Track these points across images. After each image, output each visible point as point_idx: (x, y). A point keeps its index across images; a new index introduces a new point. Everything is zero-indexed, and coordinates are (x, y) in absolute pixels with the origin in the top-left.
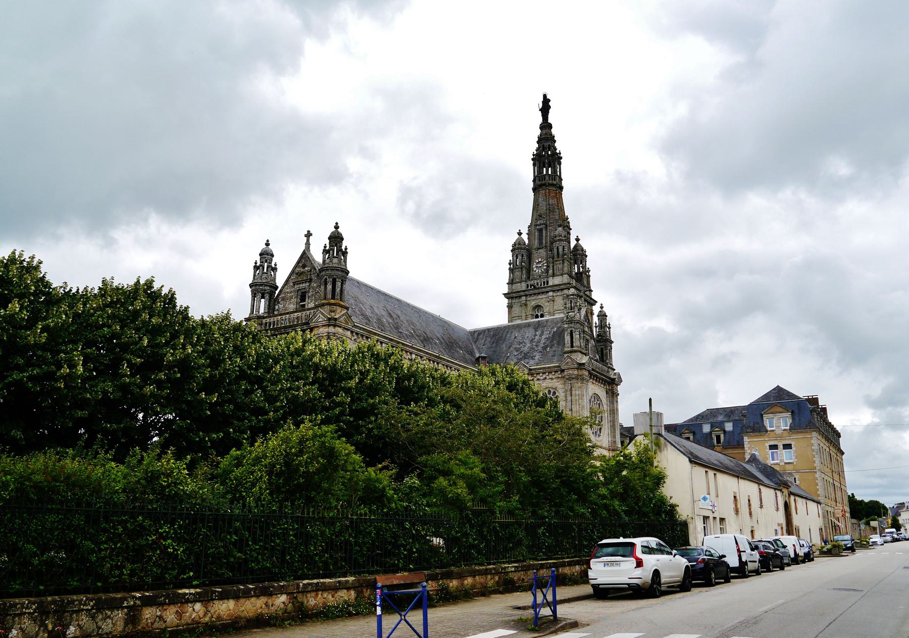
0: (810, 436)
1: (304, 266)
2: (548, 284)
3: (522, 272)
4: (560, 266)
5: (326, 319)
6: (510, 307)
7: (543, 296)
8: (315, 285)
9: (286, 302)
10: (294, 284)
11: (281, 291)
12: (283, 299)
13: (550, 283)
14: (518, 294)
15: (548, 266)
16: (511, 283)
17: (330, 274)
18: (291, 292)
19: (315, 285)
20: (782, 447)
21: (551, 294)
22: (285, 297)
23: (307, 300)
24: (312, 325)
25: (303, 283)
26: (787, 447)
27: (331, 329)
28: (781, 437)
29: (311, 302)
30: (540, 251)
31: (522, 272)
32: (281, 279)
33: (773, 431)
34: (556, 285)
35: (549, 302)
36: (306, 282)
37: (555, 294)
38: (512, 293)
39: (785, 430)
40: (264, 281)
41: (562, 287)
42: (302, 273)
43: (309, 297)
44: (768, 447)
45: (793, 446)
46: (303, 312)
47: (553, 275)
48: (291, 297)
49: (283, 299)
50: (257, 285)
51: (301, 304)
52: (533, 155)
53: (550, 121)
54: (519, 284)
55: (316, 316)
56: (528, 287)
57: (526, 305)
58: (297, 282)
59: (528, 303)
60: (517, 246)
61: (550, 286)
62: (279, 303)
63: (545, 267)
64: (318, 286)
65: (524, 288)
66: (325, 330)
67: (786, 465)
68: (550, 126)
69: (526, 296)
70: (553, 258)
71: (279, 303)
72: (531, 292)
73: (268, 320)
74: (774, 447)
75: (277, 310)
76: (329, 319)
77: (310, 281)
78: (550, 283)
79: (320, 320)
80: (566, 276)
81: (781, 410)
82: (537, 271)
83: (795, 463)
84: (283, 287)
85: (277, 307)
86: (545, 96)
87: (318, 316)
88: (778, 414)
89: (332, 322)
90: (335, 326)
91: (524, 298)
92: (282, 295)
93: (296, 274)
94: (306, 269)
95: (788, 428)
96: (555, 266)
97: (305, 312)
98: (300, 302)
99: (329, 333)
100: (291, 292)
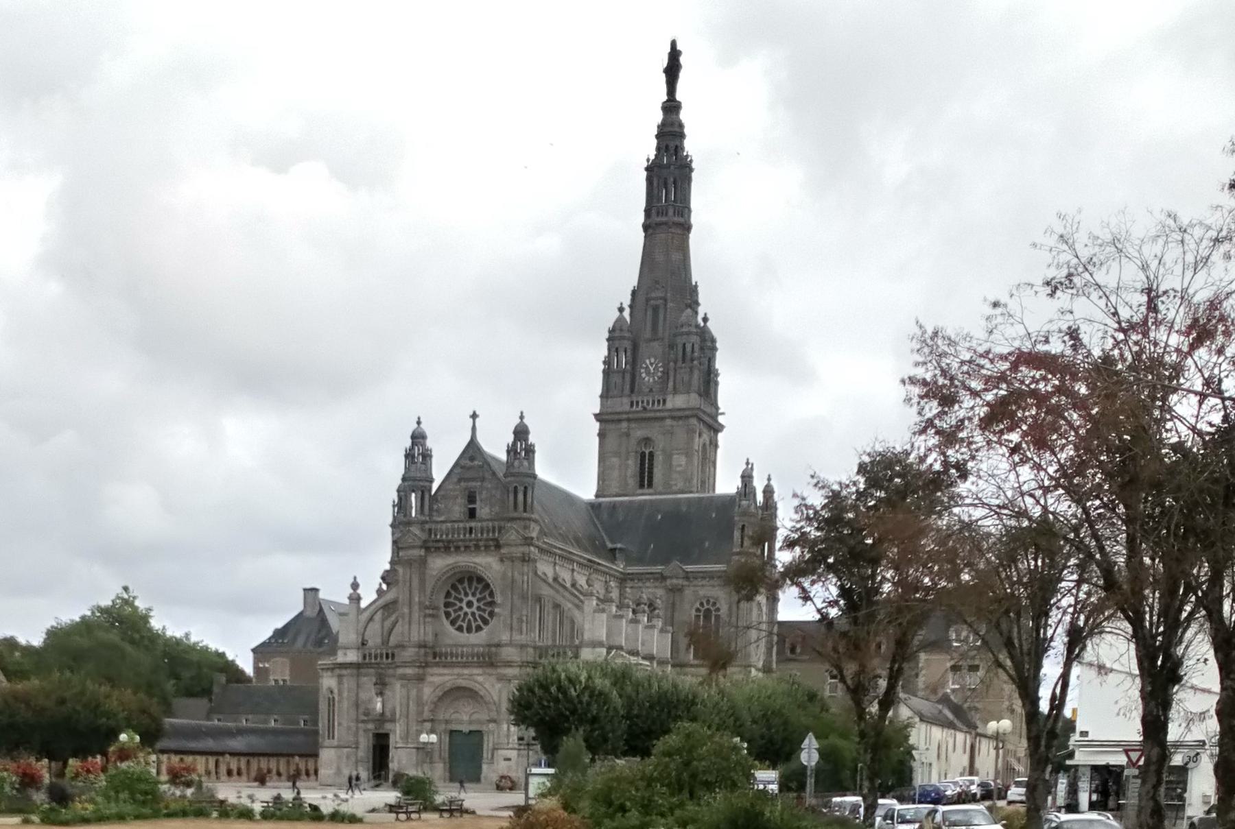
1: (472, 459)
2: (664, 401)
3: (623, 378)
4: (686, 378)
6: (602, 435)
7: (657, 424)
10: (460, 480)
11: (440, 487)
12: (444, 497)
13: (669, 405)
14: (616, 417)
15: (666, 373)
16: (604, 396)
21: (669, 422)
23: (478, 503)
27: (525, 549)
30: (653, 344)
31: (623, 378)
32: (440, 470)
34: (679, 410)
35: (664, 434)
37: (675, 423)
38: (608, 414)
40: (424, 475)
41: (687, 413)
42: (470, 468)
47: (675, 391)
49: (444, 497)
54: (619, 399)
56: (632, 405)
57: (628, 435)
59: (632, 432)
60: (617, 334)
61: (670, 410)
62: (437, 501)
63: (659, 374)
65: (627, 408)
69: (629, 420)
70: (675, 362)
71: (437, 501)
72: (636, 416)
73: (433, 526)
75: (437, 511)
76: (526, 538)
77: (483, 479)
78: (669, 405)
79: (513, 537)
80: (694, 396)
82: (646, 379)
85: (435, 507)
89: (528, 541)
90: (529, 545)
91: (624, 425)
92: (442, 493)
96: (678, 376)
99: (523, 554)
100: (455, 490)
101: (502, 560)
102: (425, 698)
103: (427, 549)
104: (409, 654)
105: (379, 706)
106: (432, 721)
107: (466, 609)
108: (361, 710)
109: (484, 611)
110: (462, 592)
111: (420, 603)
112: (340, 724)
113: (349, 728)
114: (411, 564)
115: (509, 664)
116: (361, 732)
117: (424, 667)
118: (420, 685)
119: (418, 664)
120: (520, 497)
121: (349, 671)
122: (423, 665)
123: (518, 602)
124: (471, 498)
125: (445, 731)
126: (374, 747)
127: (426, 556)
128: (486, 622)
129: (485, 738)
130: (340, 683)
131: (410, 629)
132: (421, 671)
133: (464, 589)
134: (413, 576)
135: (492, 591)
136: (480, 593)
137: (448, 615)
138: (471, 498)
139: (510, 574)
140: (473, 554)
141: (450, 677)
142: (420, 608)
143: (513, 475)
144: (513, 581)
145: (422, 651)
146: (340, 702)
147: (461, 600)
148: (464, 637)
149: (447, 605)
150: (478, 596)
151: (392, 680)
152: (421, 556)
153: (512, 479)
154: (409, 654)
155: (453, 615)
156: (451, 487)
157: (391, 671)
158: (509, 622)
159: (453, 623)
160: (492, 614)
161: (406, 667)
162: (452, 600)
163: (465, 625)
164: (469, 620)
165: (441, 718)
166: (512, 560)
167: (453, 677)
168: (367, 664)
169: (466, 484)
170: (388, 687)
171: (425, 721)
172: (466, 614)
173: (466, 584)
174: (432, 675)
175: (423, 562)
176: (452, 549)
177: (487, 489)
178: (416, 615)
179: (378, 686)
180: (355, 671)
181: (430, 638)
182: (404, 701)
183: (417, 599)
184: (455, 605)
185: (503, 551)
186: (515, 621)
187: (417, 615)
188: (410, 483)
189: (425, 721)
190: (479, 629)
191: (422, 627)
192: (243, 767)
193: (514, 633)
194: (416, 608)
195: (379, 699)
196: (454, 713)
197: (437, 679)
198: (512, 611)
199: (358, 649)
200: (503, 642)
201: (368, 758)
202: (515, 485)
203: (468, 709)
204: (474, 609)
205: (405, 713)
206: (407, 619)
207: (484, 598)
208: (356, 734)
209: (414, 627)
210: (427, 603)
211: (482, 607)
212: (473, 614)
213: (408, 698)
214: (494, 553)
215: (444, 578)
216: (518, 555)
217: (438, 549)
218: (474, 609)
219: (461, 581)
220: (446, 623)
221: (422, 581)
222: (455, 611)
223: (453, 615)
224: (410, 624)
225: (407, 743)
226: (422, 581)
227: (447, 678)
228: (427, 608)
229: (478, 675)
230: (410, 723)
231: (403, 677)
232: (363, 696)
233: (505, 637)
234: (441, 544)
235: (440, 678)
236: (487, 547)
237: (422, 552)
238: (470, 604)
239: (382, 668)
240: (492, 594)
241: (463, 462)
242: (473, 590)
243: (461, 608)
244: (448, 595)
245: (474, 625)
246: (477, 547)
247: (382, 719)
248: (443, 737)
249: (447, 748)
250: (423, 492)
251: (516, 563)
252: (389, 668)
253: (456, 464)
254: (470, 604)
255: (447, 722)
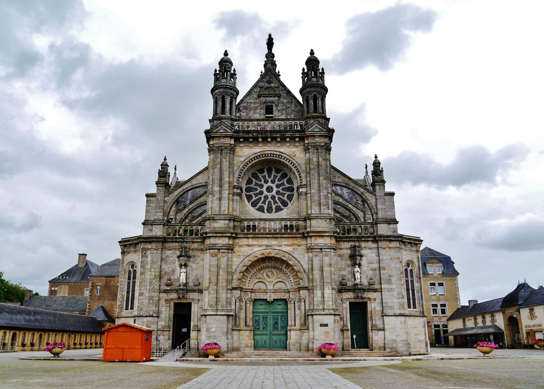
0: (454, 279)
1: (269, 82)
5: (325, 130)
8: (284, 101)
9: (249, 111)
10: (259, 96)
11: (242, 100)
12: (245, 108)
17: (319, 91)
18: (255, 103)
19: (284, 101)
20: (437, 284)
22: (248, 106)
23: (276, 114)
24: (308, 133)
25: (271, 97)
26: (441, 284)
28: (436, 278)
29: (282, 115)
33: (432, 274)
36: (275, 97)
39: (439, 274)
43: (279, 110)
44: (429, 284)
45: (444, 284)
46: (286, 122)
48: (256, 108)
49: (245, 108)
50: (227, 88)
51: (266, 115)
52: (262, 72)
53: (273, 52)
55: (313, 126)
58: (264, 94)
62: (240, 111)
64: (288, 102)
66: (322, 140)
67: (440, 296)
68: (273, 56)
71: (240, 111)
74: (433, 284)
79: (317, 130)
81: (437, 261)
83: (445, 295)
84: (245, 97)
86: (270, 35)
87: (315, 126)
88: (435, 264)
93: (260, 88)
94: (273, 85)
95: (441, 273)
97: (289, 122)
98: (266, 114)
101: (306, 150)
102: (234, 267)
103: (237, 139)
104: (220, 225)
105: (183, 276)
106: (241, 289)
107: (265, 193)
108: (164, 281)
109: (283, 195)
110: (263, 180)
111: (230, 183)
112: (141, 294)
113: (150, 298)
114: (222, 150)
115: (320, 234)
116: (163, 302)
117: (234, 238)
118: (230, 255)
119: (230, 235)
120: (319, 103)
121: (154, 245)
122: (234, 235)
123: (323, 182)
124: (269, 110)
125: (250, 300)
126: (174, 315)
127: (235, 146)
128: (285, 204)
129: (291, 306)
130: (144, 256)
131: (220, 204)
132: (231, 242)
133: (264, 177)
134: (224, 160)
135: (290, 178)
136: (279, 181)
137: (249, 198)
138: (269, 110)
139: (315, 159)
140: (279, 145)
141: (259, 249)
142: (229, 187)
143: (312, 86)
144: (318, 165)
145: (231, 224)
146: (142, 274)
147: (261, 186)
148: (266, 215)
149: (248, 190)
150: (277, 182)
151: (198, 253)
152: (231, 144)
153: (312, 89)
154: (221, 225)
155: (254, 199)
156: (252, 101)
157: (195, 246)
158: (316, 198)
159: (254, 205)
160: (290, 197)
161: (216, 237)
162: (252, 186)
163: (266, 207)
164: (270, 202)
165: (247, 287)
166: (317, 147)
167: (262, 248)
168: (172, 238)
169: (264, 99)
170: (191, 259)
171: (234, 289)
172: (266, 197)
173: (266, 173)
174: (240, 246)
175: (232, 150)
176: (260, 140)
177: (283, 103)
178: (225, 194)
179: (181, 258)
180: (160, 245)
181: (237, 213)
182: (214, 269)
183: (227, 179)
184: (257, 190)
185: (306, 142)
186: (322, 197)
187: (227, 192)
188: (221, 90)
189: (234, 289)
190: (278, 209)
191: (231, 203)
192: (36, 340)
193: (322, 207)
194: (226, 186)
195: (184, 270)
196: (258, 282)
197: (246, 250)
198: (319, 191)
199: (164, 225)
200: (312, 215)
201: (169, 327)
202: (315, 93)
203: (273, 279)
204: (274, 193)
205: (214, 280)
206: (217, 195)
207: (283, 184)
208: (158, 305)
209: (225, 203)
210: (235, 184)
211: (281, 191)
212: (273, 197)
213: (218, 267)
214: (297, 144)
215: (250, 165)
216: (322, 144)
217: (246, 140)
218: (274, 193)
219: (261, 171)
220: (248, 205)
221: (231, 165)
222: (256, 195)
223: (254, 199)
224: (220, 199)
225: (217, 310)
226: (231, 165)
227: (256, 249)
228: (235, 187)
229: (288, 246)
230: (221, 291)
231: (212, 247)
232: (166, 267)
233: (315, 211)
234: (250, 135)
235: (250, 248)
236: (292, 139)
237: (232, 142)
238: (269, 189)
239: (186, 242)
240: (290, 181)
241: (261, 84)
242: (272, 178)
243: (261, 193)
244: (249, 182)
245: (274, 207)
246: (283, 139)
247: (186, 289)
248: (248, 305)
249: (251, 315)
250: (231, 97)
251: (319, 151)
252: (193, 242)
253: (256, 86)
254: (269, 189)
255: (252, 291)
